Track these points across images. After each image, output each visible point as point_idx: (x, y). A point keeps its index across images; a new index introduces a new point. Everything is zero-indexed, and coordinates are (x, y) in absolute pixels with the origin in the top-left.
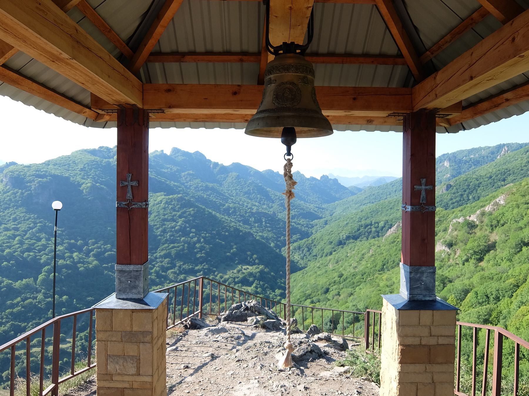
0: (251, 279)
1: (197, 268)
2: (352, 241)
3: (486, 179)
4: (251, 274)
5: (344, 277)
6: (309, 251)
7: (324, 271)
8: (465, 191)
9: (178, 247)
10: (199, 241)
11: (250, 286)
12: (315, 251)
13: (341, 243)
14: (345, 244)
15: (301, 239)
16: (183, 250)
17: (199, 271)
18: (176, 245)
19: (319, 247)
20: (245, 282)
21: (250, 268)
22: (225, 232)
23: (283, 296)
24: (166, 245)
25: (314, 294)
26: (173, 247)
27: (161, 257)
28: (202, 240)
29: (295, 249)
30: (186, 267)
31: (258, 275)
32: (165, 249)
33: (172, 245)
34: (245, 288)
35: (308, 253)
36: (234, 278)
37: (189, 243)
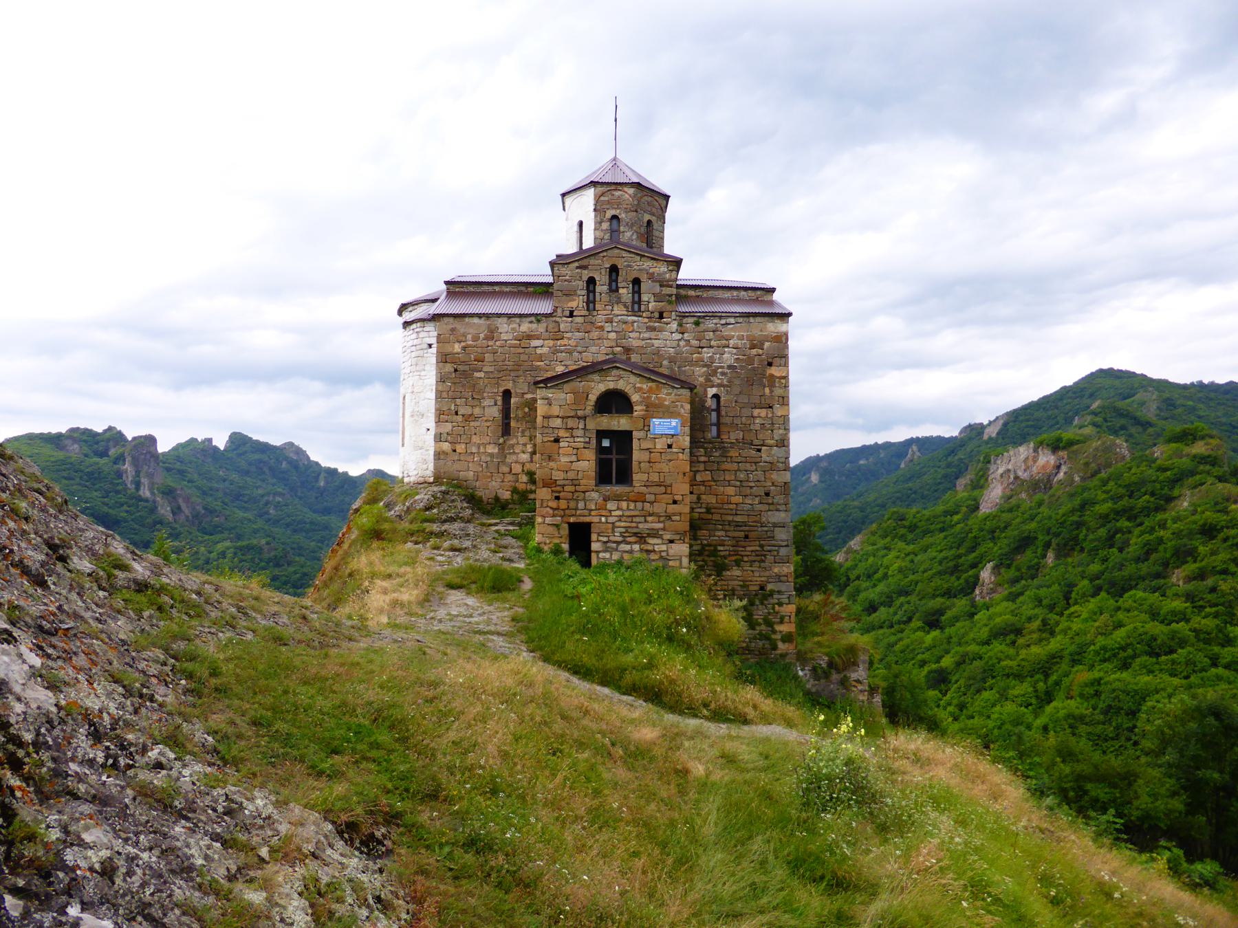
3: (876, 509)
8: (840, 532)
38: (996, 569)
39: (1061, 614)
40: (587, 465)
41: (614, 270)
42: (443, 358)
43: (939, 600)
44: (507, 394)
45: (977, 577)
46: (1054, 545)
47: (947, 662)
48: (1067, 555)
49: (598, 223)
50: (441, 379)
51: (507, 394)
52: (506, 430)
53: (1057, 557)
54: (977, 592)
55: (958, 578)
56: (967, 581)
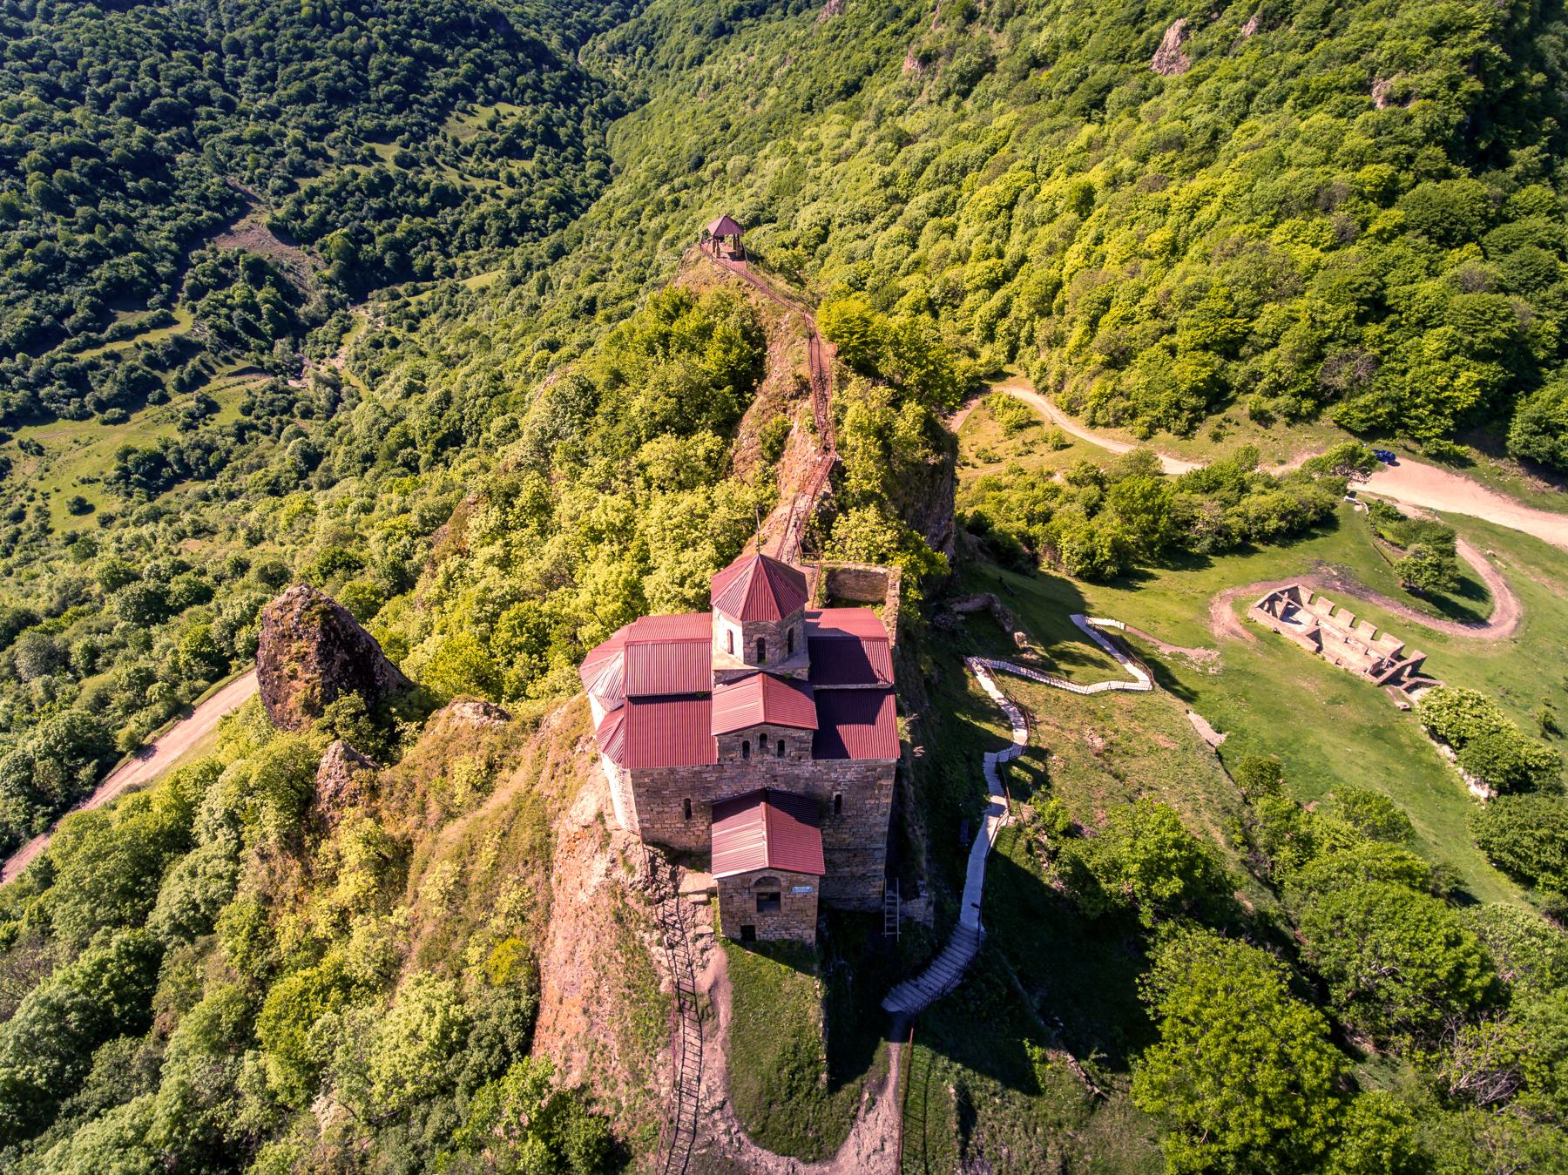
0: (526, 143)
1: (390, 124)
2: (747, 21)
4: (520, 131)
5: (733, 128)
6: (647, 54)
7: (689, 110)
9: (327, 69)
10: (374, 49)
11: (531, 156)
12: (662, 56)
13: (722, 31)
14: (731, 31)
15: (624, 18)
16: (340, 77)
17: (398, 131)
18: (318, 63)
19: (672, 41)
20: (512, 150)
21: (518, 110)
22: (433, 13)
23: (605, 178)
24: (294, 66)
25: (673, 172)
26: (315, 72)
27: (292, 101)
28: (381, 44)
29: (612, 50)
30: (368, 123)
31: (540, 129)
32: (297, 76)
33: (309, 65)
34: (517, 166)
35: (647, 60)
36: (488, 143)
37: (350, 55)
38: (1185, 31)
39: (1237, 123)
40: (752, 904)
41: (763, 738)
42: (636, 786)
43: (1109, 67)
44: (687, 802)
45: (1161, 36)
46: (1259, 12)
47: (1096, 176)
48: (1271, 28)
49: (747, 644)
50: (637, 795)
51: (687, 802)
52: (688, 815)
53: (1259, 30)
54: (1156, 58)
55: (1140, 32)
56: (1149, 40)
